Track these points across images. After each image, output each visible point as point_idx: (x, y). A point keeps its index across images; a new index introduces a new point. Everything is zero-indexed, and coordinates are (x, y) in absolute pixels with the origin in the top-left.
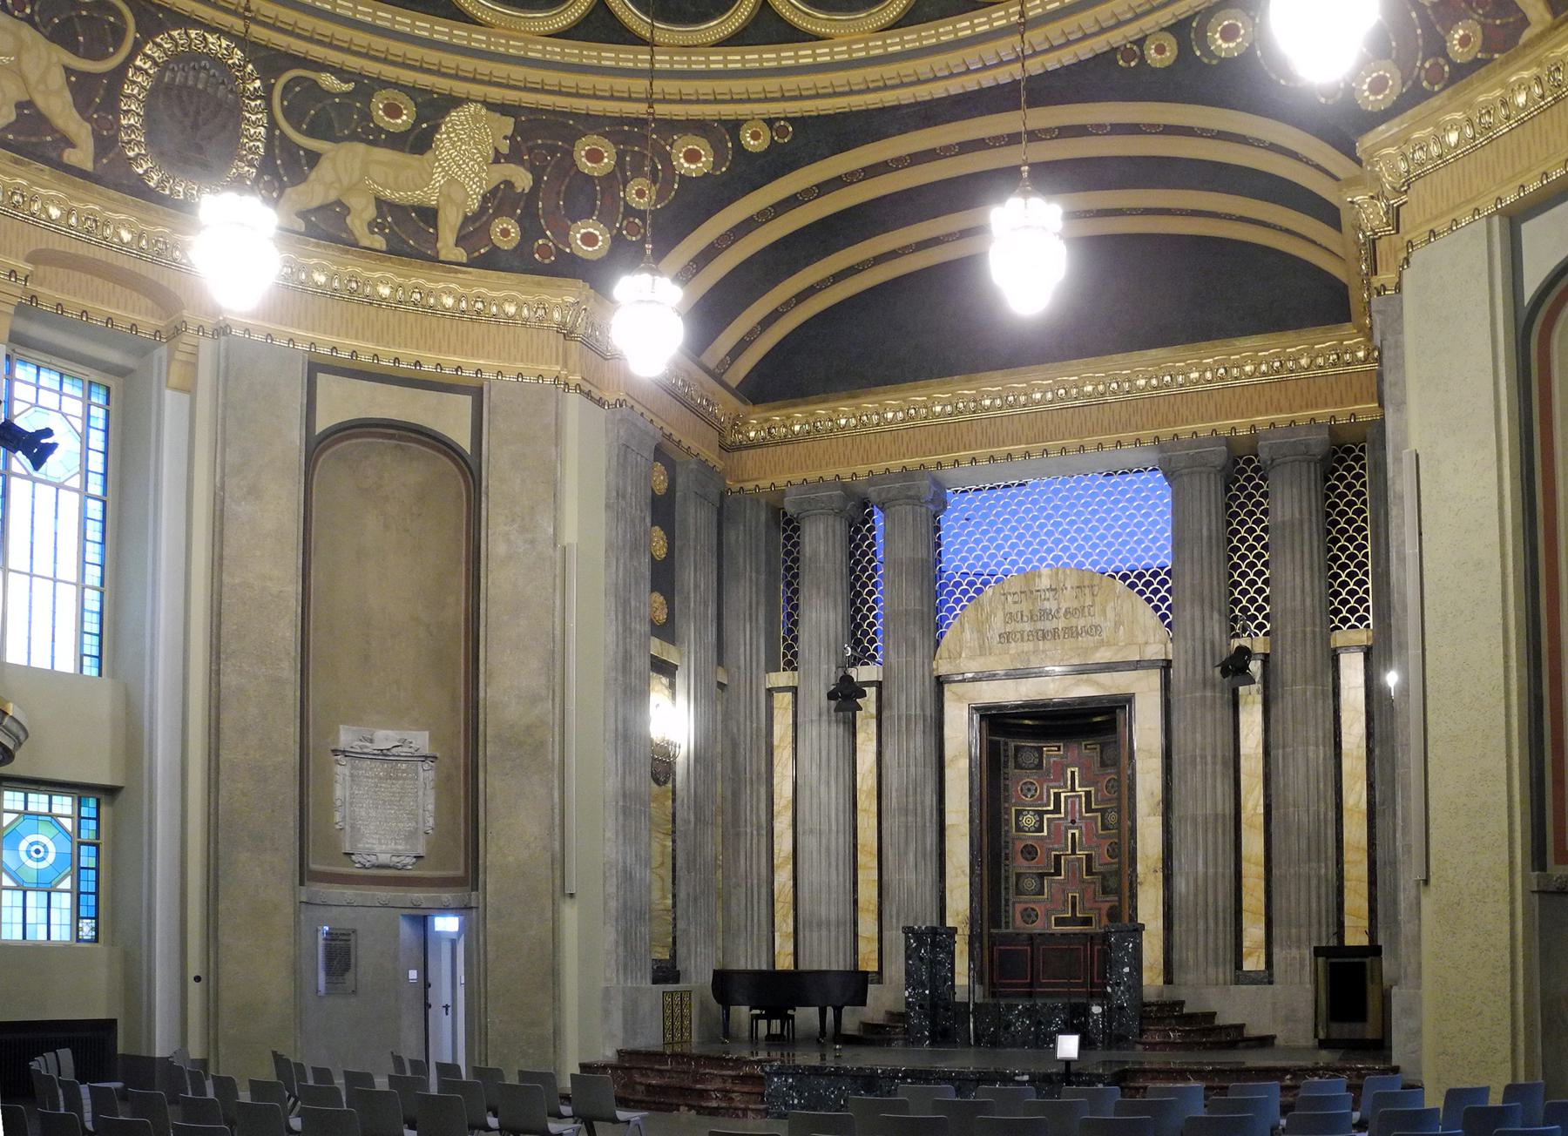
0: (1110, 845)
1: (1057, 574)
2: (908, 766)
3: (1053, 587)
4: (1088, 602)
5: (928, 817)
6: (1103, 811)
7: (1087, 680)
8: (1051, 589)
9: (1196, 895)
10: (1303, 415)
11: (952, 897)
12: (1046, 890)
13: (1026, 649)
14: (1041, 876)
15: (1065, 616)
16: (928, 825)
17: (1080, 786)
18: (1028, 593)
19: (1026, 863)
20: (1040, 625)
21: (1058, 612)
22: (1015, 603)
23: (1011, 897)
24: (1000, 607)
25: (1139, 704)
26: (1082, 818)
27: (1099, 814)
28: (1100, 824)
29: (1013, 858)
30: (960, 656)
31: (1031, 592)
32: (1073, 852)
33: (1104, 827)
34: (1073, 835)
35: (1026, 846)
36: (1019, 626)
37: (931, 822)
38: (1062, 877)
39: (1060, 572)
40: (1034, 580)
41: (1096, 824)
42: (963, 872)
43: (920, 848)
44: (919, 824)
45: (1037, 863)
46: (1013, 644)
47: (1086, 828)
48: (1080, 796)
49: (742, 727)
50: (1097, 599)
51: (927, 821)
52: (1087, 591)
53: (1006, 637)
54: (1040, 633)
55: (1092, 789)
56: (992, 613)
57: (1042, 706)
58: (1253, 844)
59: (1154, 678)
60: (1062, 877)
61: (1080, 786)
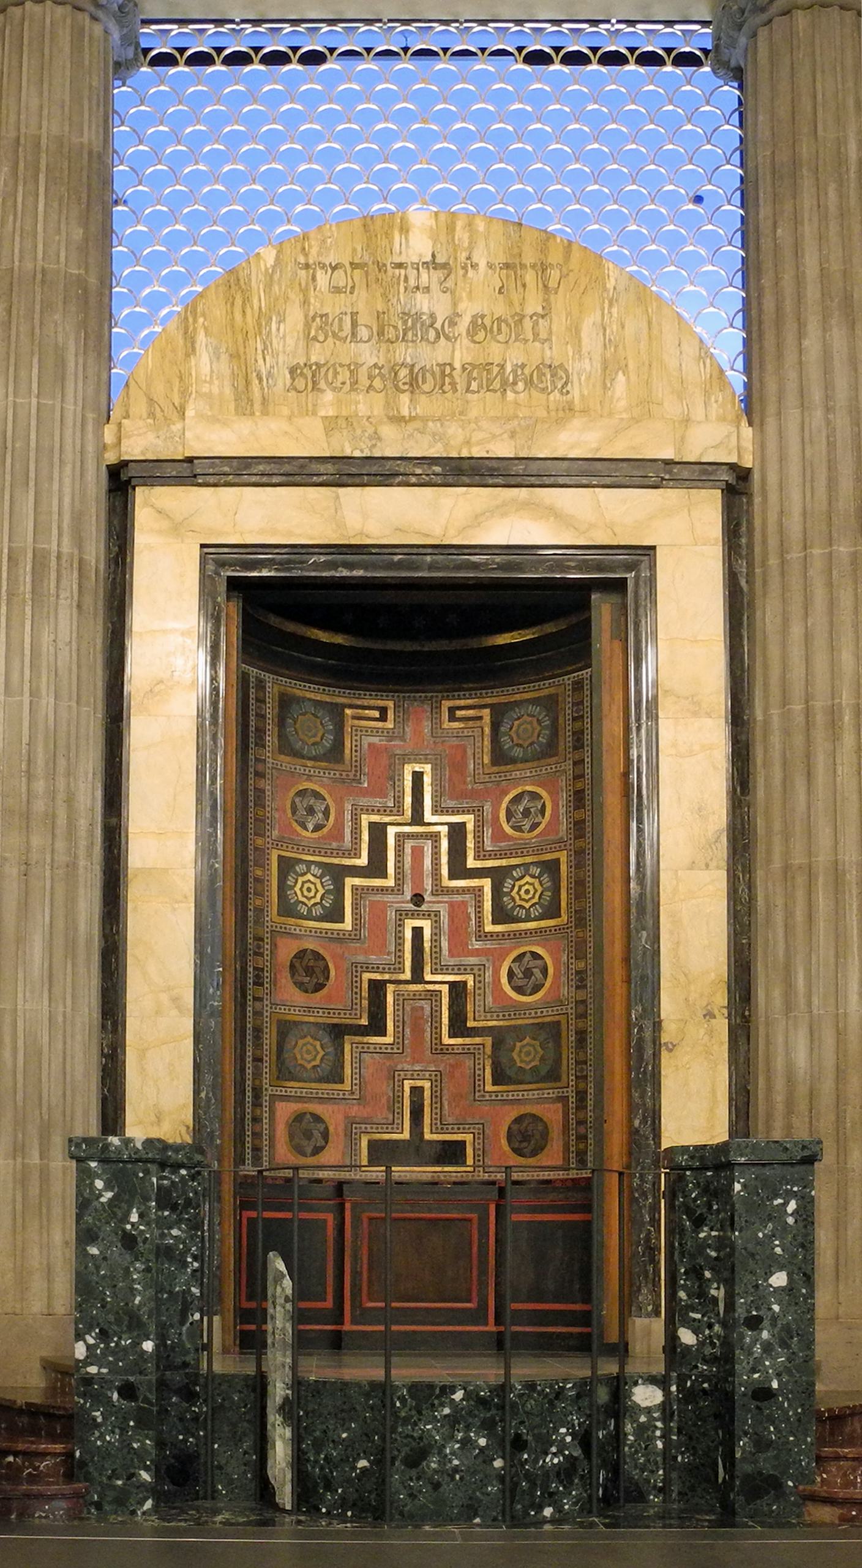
0: (519, 958)
1: (451, 229)
2: (34, 693)
3: (440, 259)
5: (83, 843)
6: (498, 876)
8: (433, 264)
11: (142, 1070)
12: (348, 1071)
14: (338, 1032)
16: (82, 863)
17: (435, 812)
18: (373, 268)
19: (298, 997)
20: (403, 353)
22: (337, 290)
23: (266, 1082)
24: (296, 297)
26: (439, 890)
27: (487, 884)
28: (488, 905)
29: (274, 982)
30: (182, 412)
31: (381, 267)
32: (418, 976)
33: (501, 915)
34: (418, 932)
35: (301, 954)
36: (347, 352)
37: (90, 855)
38: (389, 1039)
39: (459, 224)
40: (388, 236)
41: (479, 906)
42: (176, 1000)
43: (60, 924)
44: (62, 858)
45: (329, 998)
46: (329, 396)
47: (452, 918)
48: (435, 837)
51: (82, 852)
54: (403, 373)
55: (469, 819)
56: (275, 311)
60: (389, 1039)
61: (435, 812)
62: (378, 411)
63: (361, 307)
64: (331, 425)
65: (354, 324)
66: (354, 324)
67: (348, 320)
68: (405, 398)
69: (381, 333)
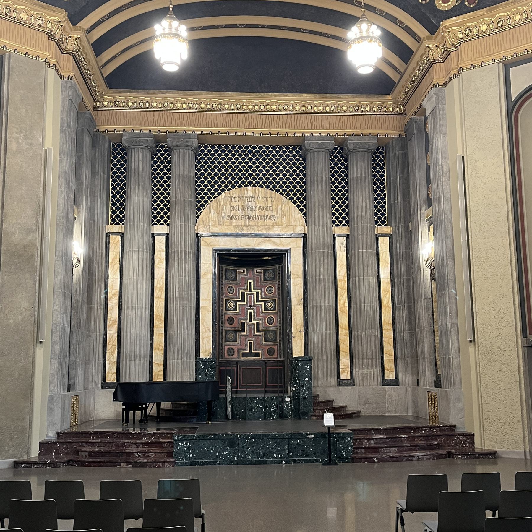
3: (253, 196)
4: (269, 205)
7: (268, 241)
9: (322, 343)
10: (366, 132)
13: (240, 224)
15: (259, 210)
18: (242, 198)
20: (247, 213)
21: (256, 208)
24: (228, 203)
25: (292, 252)
31: (243, 197)
36: (237, 213)
49: (95, 252)
50: (274, 203)
52: (269, 199)
53: (231, 217)
57: (246, 251)
58: (344, 320)
59: (300, 241)
62: (243, 224)
63: (240, 205)
64: (235, 227)
65: (239, 208)
66: (239, 208)
67: (237, 207)
68: (247, 221)
69: (243, 209)
